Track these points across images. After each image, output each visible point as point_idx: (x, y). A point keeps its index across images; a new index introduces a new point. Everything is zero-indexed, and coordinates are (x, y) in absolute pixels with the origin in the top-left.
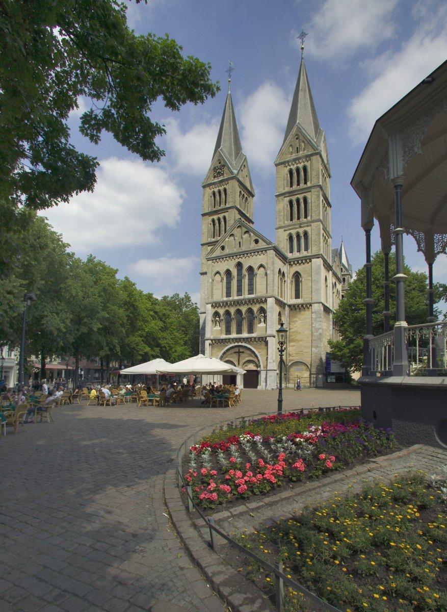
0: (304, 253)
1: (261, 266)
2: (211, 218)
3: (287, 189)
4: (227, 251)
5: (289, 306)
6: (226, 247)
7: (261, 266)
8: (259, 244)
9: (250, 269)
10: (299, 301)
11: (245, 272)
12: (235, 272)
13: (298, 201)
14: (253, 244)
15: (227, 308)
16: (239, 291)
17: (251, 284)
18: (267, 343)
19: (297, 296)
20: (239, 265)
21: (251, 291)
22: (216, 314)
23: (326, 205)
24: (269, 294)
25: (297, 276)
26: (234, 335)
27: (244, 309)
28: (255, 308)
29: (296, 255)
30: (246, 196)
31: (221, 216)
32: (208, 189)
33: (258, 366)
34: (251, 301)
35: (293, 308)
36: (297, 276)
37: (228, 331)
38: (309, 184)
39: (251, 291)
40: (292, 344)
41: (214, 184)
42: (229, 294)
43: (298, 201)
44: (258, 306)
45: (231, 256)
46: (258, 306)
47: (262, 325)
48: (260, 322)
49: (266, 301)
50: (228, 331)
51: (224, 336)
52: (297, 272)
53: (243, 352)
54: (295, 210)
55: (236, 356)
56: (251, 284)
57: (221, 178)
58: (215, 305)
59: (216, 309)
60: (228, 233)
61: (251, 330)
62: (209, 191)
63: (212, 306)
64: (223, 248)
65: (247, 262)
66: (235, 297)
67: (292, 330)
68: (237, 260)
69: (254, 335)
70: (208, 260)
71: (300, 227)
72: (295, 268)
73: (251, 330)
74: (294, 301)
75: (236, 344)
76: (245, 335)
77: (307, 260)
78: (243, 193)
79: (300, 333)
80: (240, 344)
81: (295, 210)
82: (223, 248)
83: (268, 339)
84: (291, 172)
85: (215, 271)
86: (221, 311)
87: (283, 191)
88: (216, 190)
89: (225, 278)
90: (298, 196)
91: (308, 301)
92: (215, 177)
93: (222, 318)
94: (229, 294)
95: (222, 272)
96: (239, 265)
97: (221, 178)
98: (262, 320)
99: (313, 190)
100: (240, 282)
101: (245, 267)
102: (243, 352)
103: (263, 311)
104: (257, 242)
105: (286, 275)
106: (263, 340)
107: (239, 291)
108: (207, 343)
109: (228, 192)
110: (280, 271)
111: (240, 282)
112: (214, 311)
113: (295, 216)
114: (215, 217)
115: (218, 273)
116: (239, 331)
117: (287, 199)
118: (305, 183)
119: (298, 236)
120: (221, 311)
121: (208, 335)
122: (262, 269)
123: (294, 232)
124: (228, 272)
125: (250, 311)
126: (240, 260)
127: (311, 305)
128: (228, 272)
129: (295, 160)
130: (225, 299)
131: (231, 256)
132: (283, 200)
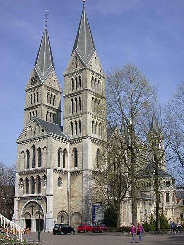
0: (79, 135)
1: (45, 147)
3: (70, 92)
4: (28, 137)
5: (70, 172)
9: (39, 149)
10: (76, 169)
11: (37, 152)
15: (26, 176)
16: (34, 165)
17: (40, 159)
18: (46, 199)
19: (76, 166)
20: (34, 147)
21: (40, 165)
22: (21, 180)
23: (98, 99)
24: (48, 166)
25: (75, 151)
26: (30, 195)
27: (35, 176)
29: (75, 136)
30: (53, 94)
31: (34, 110)
32: (28, 92)
33: (43, 216)
34: (39, 171)
35: (72, 173)
36: (75, 151)
37: (27, 192)
39: (40, 165)
40: (72, 199)
42: (28, 167)
45: (29, 140)
46: (42, 174)
47: (44, 187)
50: (27, 192)
51: (25, 195)
52: (75, 148)
53: (35, 206)
54: (75, 106)
55: (31, 208)
56: (40, 159)
57: (35, 85)
58: (21, 174)
59: (21, 176)
61: (39, 192)
62: (29, 93)
66: (31, 168)
67: (72, 190)
68: (32, 144)
69: (41, 194)
70: (18, 143)
71: (77, 117)
72: (74, 146)
73: (39, 192)
74: (74, 169)
75: (31, 200)
76: (36, 194)
77: (80, 140)
78: (50, 93)
79: (77, 191)
80: (33, 200)
81: (75, 106)
82: (26, 135)
85: (21, 151)
86: (24, 178)
87: (68, 93)
88: (32, 93)
89: (26, 156)
90: (76, 96)
91: (81, 168)
93: (24, 182)
94: (28, 167)
96: (34, 147)
97: (35, 85)
99: (83, 92)
100: (34, 157)
101: (37, 148)
102: (35, 206)
103: (45, 177)
105: (68, 151)
106: (44, 198)
107: (34, 165)
108: (15, 199)
109: (39, 94)
110: (60, 149)
111: (34, 157)
114: (31, 111)
115: (23, 152)
116: (33, 192)
119: (76, 122)
120: (24, 178)
121: (17, 194)
123: (73, 121)
124: (28, 152)
125: (39, 178)
127: (82, 172)
129: (74, 73)
130: (26, 169)
131: (29, 140)
132: (67, 99)
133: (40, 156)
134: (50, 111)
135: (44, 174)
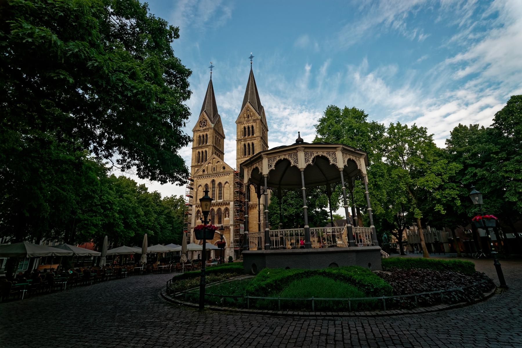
1: (227, 182)
2: (197, 151)
6: (206, 170)
7: (227, 182)
8: (226, 169)
9: (220, 184)
12: (210, 185)
13: (249, 144)
14: (222, 170)
17: (220, 193)
20: (213, 181)
27: (216, 209)
28: (223, 208)
30: (219, 138)
38: (255, 135)
39: (220, 198)
41: (199, 130)
43: (249, 144)
44: (225, 207)
46: (225, 207)
47: (227, 219)
48: (225, 217)
49: (229, 203)
56: (220, 193)
57: (205, 128)
60: (207, 162)
63: (196, 206)
64: (204, 171)
65: (218, 180)
68: (212, 178)
82: (204, 171)
83: (230, 227)
84: (245, 128)
90: (249, 142)
92: (200, 127)
95: (203, 185)
96: (213, 181)
98: (227, 215)
103: (227, 210)
104: (224, 168)
112: (197, 209)
113: (247, 153)
114: (200, 150)
115: (200, 185)
117: (243, 143)
118: (253, 135)
122: (227, 184)
124: (206, 185)
125: (219, 210)
126: (214, 178)
128: (206, 185)
131: (208, 175)
133: (220, 190)
134: (217, 152)
135: (227, 206)
